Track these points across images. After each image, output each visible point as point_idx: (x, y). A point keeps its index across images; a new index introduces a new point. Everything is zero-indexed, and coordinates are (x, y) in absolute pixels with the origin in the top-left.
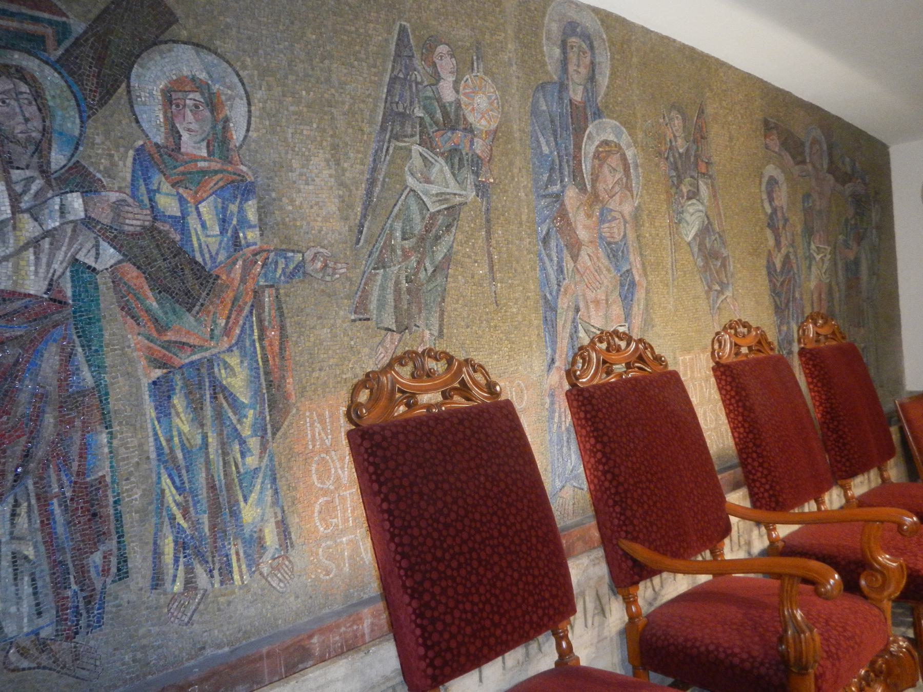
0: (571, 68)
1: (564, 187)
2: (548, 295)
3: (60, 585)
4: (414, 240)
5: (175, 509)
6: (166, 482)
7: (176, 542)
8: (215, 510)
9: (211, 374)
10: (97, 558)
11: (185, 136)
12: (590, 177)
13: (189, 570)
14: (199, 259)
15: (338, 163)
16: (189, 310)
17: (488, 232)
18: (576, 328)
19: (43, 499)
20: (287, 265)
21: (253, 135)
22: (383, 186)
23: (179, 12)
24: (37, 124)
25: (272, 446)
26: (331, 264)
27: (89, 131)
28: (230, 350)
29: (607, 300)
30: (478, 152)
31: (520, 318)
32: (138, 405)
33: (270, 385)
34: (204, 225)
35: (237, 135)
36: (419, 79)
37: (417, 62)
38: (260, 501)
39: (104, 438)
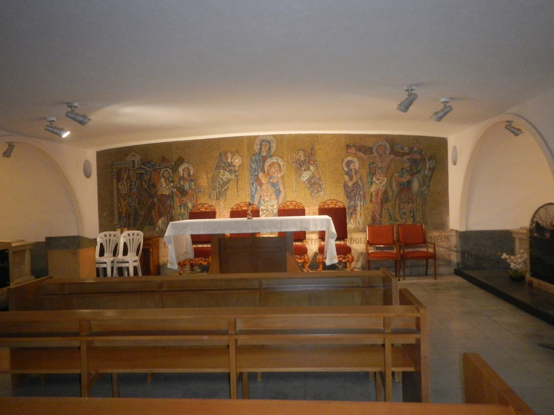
0: (263, 149)
1: (258, 174)
2: (252, 194)
6: (180, 217)
9: (186, 205)
12: (267, 171)
15: (207, 175)
16: (184, 196)
17: (237, 183)
19: (167, 217)
23: (185, 159)
26: (205, 190)
28: (189, 202)
29: (271, 195)
31: (244, 198)
35: (192, 173)
39: (174, 211)
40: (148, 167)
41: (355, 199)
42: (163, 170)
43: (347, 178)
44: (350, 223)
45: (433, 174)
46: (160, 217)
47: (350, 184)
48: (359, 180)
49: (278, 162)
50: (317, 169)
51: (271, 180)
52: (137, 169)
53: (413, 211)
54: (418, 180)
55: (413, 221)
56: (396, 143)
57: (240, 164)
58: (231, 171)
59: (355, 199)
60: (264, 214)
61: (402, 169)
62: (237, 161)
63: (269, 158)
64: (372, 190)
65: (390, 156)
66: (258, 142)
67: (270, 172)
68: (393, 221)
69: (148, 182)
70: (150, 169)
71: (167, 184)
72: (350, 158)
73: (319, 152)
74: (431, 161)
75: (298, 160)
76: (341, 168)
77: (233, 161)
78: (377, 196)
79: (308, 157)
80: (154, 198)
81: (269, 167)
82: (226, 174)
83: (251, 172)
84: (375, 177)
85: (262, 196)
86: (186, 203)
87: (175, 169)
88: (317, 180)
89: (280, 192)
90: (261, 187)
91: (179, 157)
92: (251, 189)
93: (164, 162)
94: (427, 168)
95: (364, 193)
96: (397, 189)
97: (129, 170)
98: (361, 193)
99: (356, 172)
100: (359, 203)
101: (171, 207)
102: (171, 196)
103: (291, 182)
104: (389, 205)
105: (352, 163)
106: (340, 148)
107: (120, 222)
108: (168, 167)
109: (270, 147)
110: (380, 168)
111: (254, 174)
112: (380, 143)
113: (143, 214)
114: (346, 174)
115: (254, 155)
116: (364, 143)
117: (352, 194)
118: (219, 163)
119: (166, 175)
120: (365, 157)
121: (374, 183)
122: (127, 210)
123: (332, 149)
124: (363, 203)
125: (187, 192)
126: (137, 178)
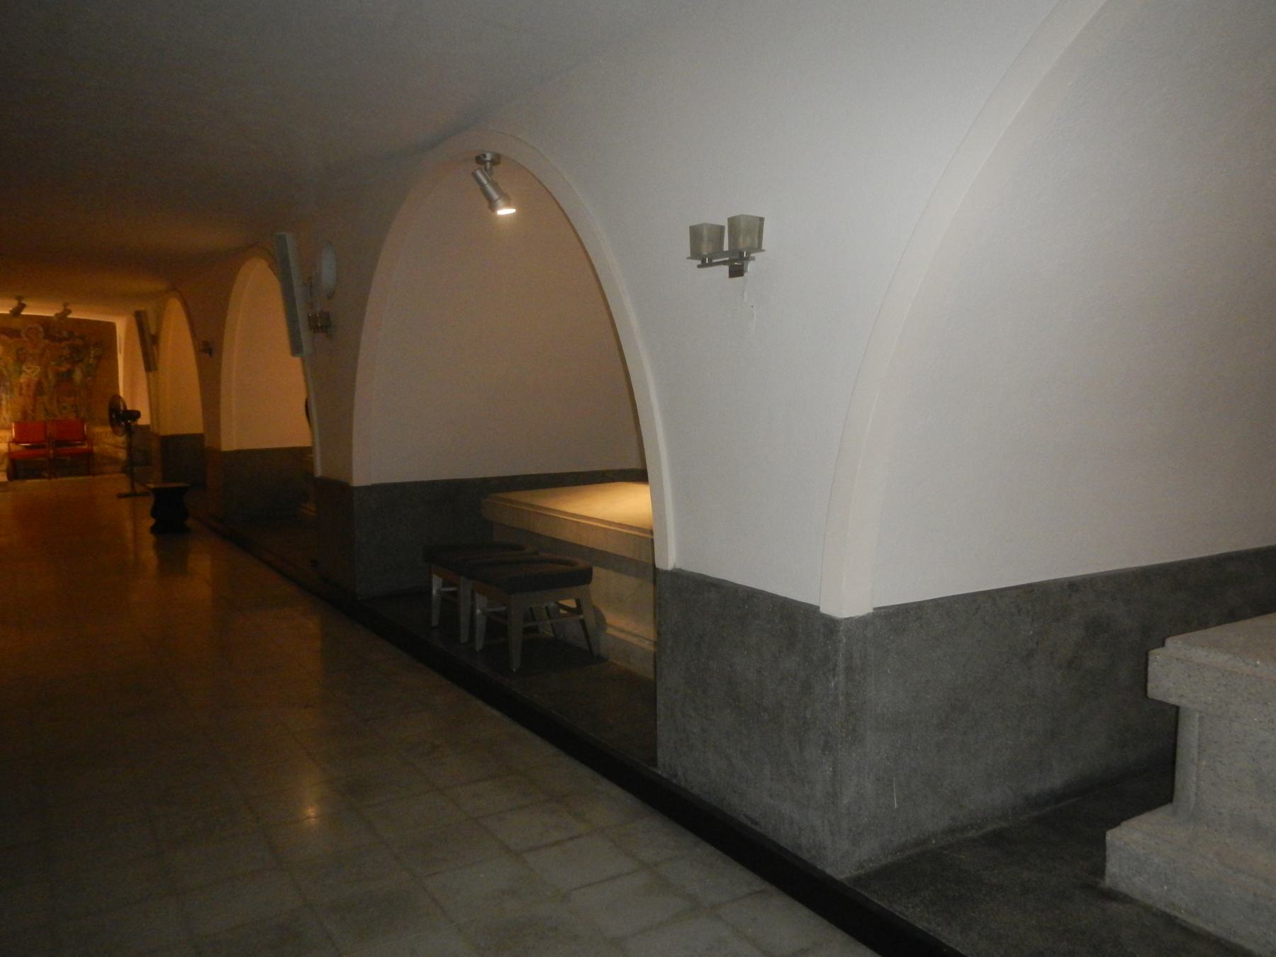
94: (92, 356)
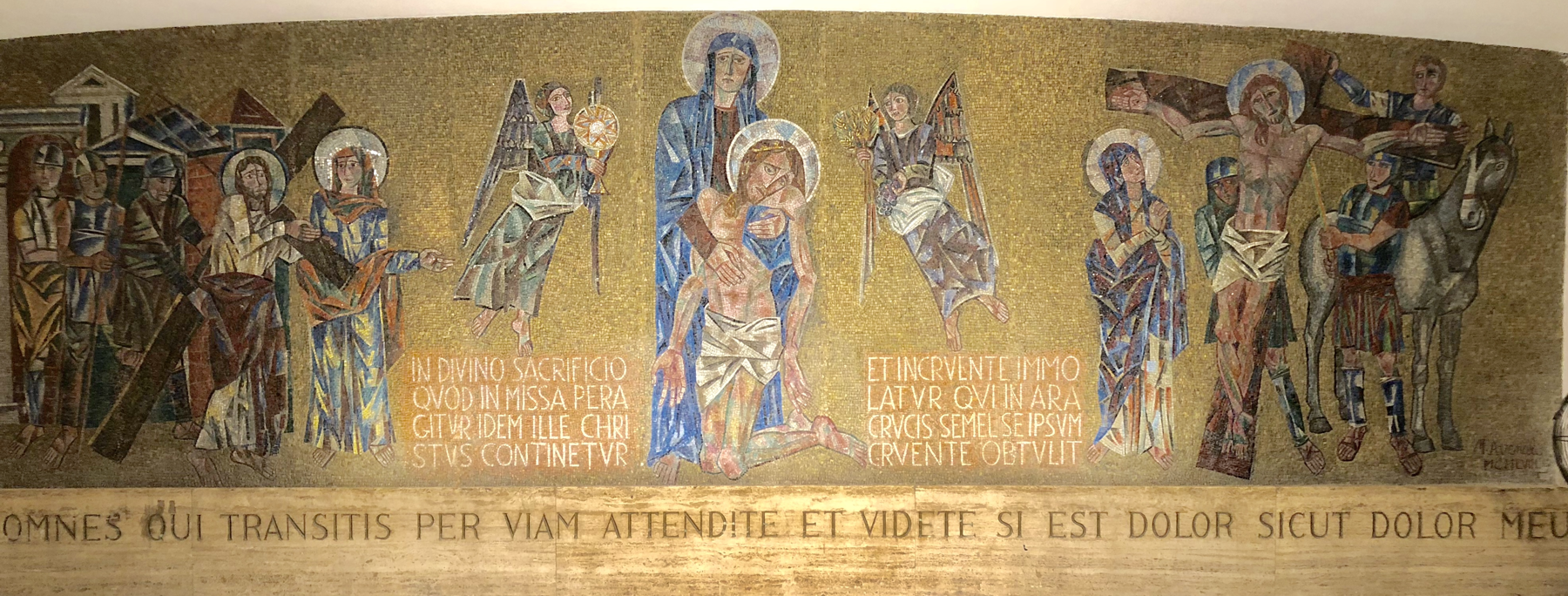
0: (718, 79)
2: (666, 288)
3: (259, 426)
4: (515, 242)
5: (321, 401)
6: (317, 385)
7: (320, 419)
8: (346, 406)
9: (350, 327)
10: (278, 417)
11: (344, 184)
13: (327, 437)
14: (347, 257)
18: (701, 319)
19: (255, 382)
20: (406, 261)
21: (389, 178)
22: (490, 204)
23: (345, 110)
24: (264, 186)
25: (385, 375)
26: (440, 260)
27: (290, 187)
28: (363, 312)
29: (750, 294)
30: (590, 169)
32: (306, 338)
33: (387, 337)
34: (352, 237)
35: (377, 181)
36: (531, 119)
37: (531, 107)
38: (374, 407)
40: (167, 141)
41: (1137, 322)
42: (241, 156)
43: (1103, 225)
44: (1110, 432)
45: (1497, 219)
46: (220, 383)
47: (1118, 254)
48: (1161, 237)
49: (787, 143)
50: (969, 180)
51: (755, 227)
52: (107, 147)
53: (1400, 384)
54: (1427, 241)
55: (1394, 427)
56: (1331, 71)
57: (610, 145)
58: (565, 178)
59: (1137, 322)
60: (717, 379)
61: (1358, 192)
62: (597, 132)
63: (749, 120)
64: (1215, 283)
65: (1301, 129)
66: (696, 43)
67: (753, 189)
68: (1307, 427)
69: (162, 213)
70: (177, 153)
71: (257, 227)
72: (1119, 136)
73: (982, 100)
74: (1488, 161)
75: (882, 134)
76: (1079, 179)
77: (577, 128)
78: (1240, 313)
79: (930, 123)
80: (192, 289)
81: (748, 164)
82: (542, 189)
83: (660, 184)
84: (1233, 225)
85: (711, 297)
86: (349, 319)
87: (298, 152)
88: (965, 230)
89: (795, 278)
90: (705, 255)
91: (316, 98)
92: (661, 264)
93: (246, 121)
95: (1182, 299)
96: (1331, 281)
97: (69, 147)
98: (1166, 297)
99: (1148, 201)
100: (1154, 341)
101: (276, 334)
102: (272, 286)
103: (847, 236)
104: (1292, 356)
105: (1132, 159)
106: (1078, 86)
107: (19, 398)
108: (265, 144)
109: (753, 70)
110: (1258, 185)
111: (677, 195)
112: (1263, 70)
113: (135, 362)
114: (1100, 208)
115: (677, 102)
116: (1190, 68)
117: (1126, 302)
118: (508, 136)
119: (254, 182)
120: (1191, 131)
121: (1228, 254)
122: (57, 340)
123: (1040, 92)
124: (1175, 341)
125: (351, 269)
126: (108, 193)
